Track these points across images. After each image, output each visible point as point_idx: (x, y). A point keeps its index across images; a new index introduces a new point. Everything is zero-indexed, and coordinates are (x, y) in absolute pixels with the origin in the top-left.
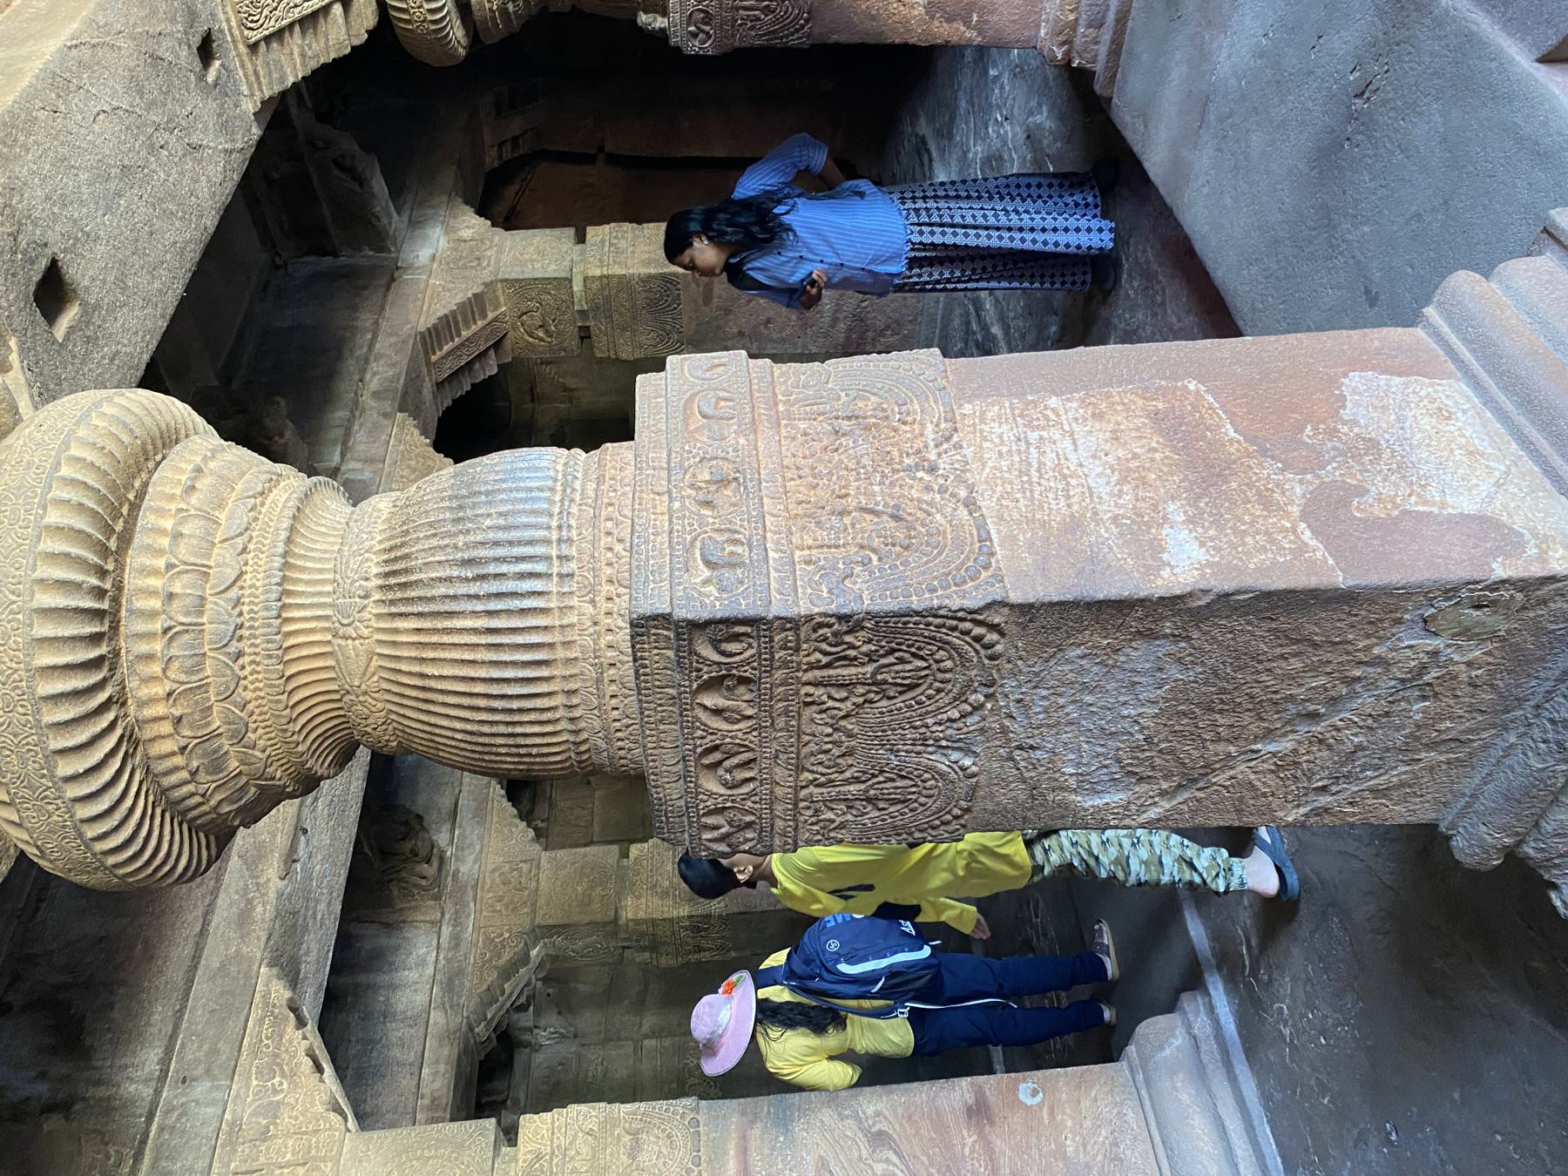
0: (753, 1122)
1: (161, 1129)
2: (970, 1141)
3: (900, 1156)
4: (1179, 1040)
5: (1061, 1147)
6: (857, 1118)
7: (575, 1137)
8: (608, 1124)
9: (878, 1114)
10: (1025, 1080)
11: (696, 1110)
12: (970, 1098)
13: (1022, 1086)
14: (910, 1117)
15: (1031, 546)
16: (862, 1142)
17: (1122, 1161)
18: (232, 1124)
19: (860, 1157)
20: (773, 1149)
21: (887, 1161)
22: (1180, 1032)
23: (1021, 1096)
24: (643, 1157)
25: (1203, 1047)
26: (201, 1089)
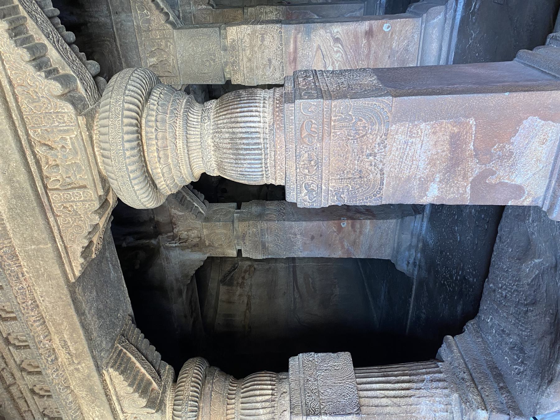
0: (299, 33)
1: (117, 29)
2: (364, 42)
4: (441, 17)
5: (391, 45)
6: (331, 33)
7: (244, 36)
8: (254, 32)
9: (337, 32)
10: (387, 23)
11: (281, 28)
12: (367, 28)
13: (385, 25)
15: (394, 185)
16: (332, 41)
17: (408, 51)
20: (304, 41)
22: (442, 14)
23: (384, 28)
25: (447, 22)
26: (123, 16)
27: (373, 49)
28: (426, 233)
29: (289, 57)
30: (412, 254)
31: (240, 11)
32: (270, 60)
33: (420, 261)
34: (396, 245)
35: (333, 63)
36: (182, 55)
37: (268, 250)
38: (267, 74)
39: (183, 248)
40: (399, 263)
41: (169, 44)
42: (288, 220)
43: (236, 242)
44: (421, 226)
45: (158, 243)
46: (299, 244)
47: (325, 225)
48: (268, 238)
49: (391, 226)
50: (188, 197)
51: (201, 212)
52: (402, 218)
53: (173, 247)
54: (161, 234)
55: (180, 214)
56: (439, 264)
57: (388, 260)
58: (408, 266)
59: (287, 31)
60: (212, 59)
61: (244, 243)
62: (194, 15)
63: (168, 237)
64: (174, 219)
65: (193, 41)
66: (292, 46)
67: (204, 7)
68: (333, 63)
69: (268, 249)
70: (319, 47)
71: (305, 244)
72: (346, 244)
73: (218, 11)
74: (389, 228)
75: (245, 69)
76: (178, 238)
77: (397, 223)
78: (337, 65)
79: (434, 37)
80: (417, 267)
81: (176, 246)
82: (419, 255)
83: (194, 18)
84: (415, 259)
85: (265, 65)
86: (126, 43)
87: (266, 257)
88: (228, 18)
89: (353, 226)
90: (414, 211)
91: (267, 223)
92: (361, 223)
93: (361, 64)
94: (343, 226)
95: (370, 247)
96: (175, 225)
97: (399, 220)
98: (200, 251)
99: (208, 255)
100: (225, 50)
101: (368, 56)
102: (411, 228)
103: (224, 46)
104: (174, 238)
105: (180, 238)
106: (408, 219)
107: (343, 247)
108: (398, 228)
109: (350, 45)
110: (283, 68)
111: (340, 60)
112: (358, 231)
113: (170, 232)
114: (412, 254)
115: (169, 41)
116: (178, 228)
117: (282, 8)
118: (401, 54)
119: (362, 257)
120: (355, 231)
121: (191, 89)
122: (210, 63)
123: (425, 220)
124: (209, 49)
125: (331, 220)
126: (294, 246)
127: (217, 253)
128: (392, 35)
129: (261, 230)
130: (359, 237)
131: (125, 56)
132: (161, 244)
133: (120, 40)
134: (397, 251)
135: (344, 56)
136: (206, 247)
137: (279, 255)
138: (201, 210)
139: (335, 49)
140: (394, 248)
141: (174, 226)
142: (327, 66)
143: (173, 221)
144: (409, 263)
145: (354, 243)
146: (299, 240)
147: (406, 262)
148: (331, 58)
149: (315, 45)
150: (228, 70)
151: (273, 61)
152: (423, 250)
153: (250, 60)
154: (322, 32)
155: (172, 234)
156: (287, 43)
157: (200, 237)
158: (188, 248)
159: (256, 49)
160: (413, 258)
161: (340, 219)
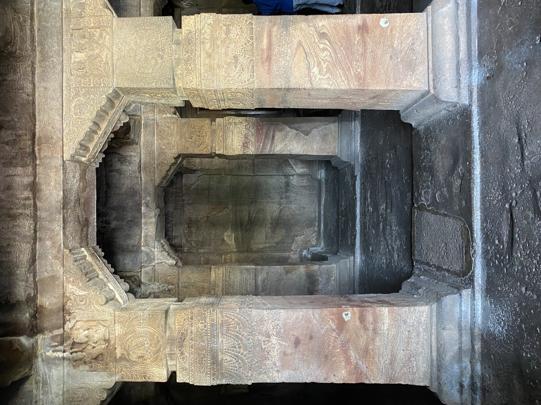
0: (274, 25)
1: (39, 10)
3: (330, 42)
6: (315, 26)
7: (204, 26)
9: (323, 26)
10: (383, 17)
11: (252, 18)
12: (360, 22)
13: (382, 20)
14: (336, 28)
17: (414, 50)
18: (67, 10)
19: (315, 41)
20: (281, 36)
21: (325, 44)
24: (231, 35)
25: (460, 8)
27: (369, 47)
28: (485, 318)
29: (262, 55)
30: (466, 367)
31: (208, 121)
32: (236, 58)
33: (483, 379)
34: (434, 354)
35: (319, 63)
36: (119, 49)
37: (221, 369)
38: (232, 75)
39: (76, 362)
40: (445, 389)
41: (104, 34)
42: (257, 308)
43: (168, 350)
44: (473, 310)
45: (34, 347)
46: (275, 354)
47: (317, 316)
48: (223, 343)
49: (423, 319)
50: (100, 273)
51: (117, 300)
52: (438, 299)
53: (58, 358)
54: (41, 331)
55: (82, 293)
56: (533, 358)
57: (425, 388)
58: (461, 391)
59: (260, 23)
60: (159, 56)
61: (182, 354)
62: (157, 123)
63: (53, 338)
64: (69, 304)
65: (136, 31)
66: (265, 41)
67: (168, 115)
68: (319, 63)
69: (221, 364)
70: (300, 44)
71: (285, 354)
72: (352, 353)
73: (184, 120)
74: (419, 323)
75: (202, 68)
76: (70, 342)
77: (431, 312)
78: (325, 66)
79: (446, 28)
80: (479, 393)
81: (64, 358)
82: (478, 367)
83: (157, 126)
84: (472, 378)
85: (229, 64)
86: (47, 27)
87: (219, 382)
88: (194, 128)
89: (362, 319)
90: (456, 288)
91: (221, 312)
92: (374, 312)
93: (356, 65)
94: (346, 318)
95: (392, 363)
96: (70, 314)
97: (435, 306)
98: (104, 370)
99: (117, 378)
100: (178, 43)
101: (364, 55)
102: (457, 316)
103: (178, 40)
104: (63, 339)
105: (74, 343)
106: (449, 300)
107: (348, 360)
108: (434, 319)
109: (340, 42)
110: (253, 67)
111: (328, 59)
112: (371, 327)
113: (59, 328)
114: (466, 367)
115: (105, 30)
116: (73, 321)
117: (252, 119)
118: (405, 54)
119: (382, 382)
120: (366, 329)
121: (143, 202)
122: (156, 60)
123: (478, 296)
124: (157, 43)
125: (327, 308)
126: (266, 358)
127: (134, 375)
128: (391, 31)
129: (212, 325)
130: (373, 340)
131: (41, 44)
132: (39, 353)
133: (40, 21)
134: (438, 366)
135: (332, 55)
136: (116, 360)
137: (240, 376)
138: (118, 296)
139: (321, 46)
140: (432, 360)
141: (68, 318)
142: (312, 67)
143: (67, 307)
144: (462, 386)
145: (366, 353)
146: (276, 346)
147: (458, 387)
148: (316, 57)
149: (296, 41)
150: (179, 72)
151: (241, 59)
152: (486, 356)
153: (210, 56)
154: (303, 25)
155: (61, 331)
156: (259, 38)
157: (107, 341)
158: (85, 363)
159: (219, 42)
160: (468, 376)
161: (341, 307)
